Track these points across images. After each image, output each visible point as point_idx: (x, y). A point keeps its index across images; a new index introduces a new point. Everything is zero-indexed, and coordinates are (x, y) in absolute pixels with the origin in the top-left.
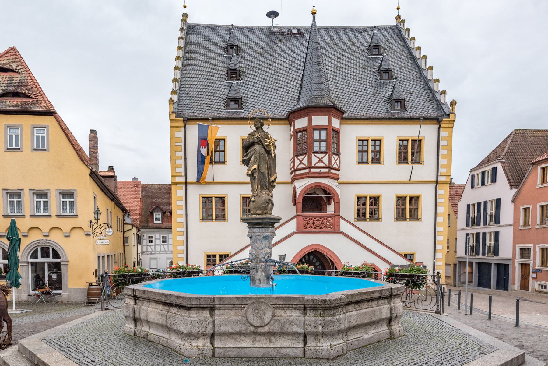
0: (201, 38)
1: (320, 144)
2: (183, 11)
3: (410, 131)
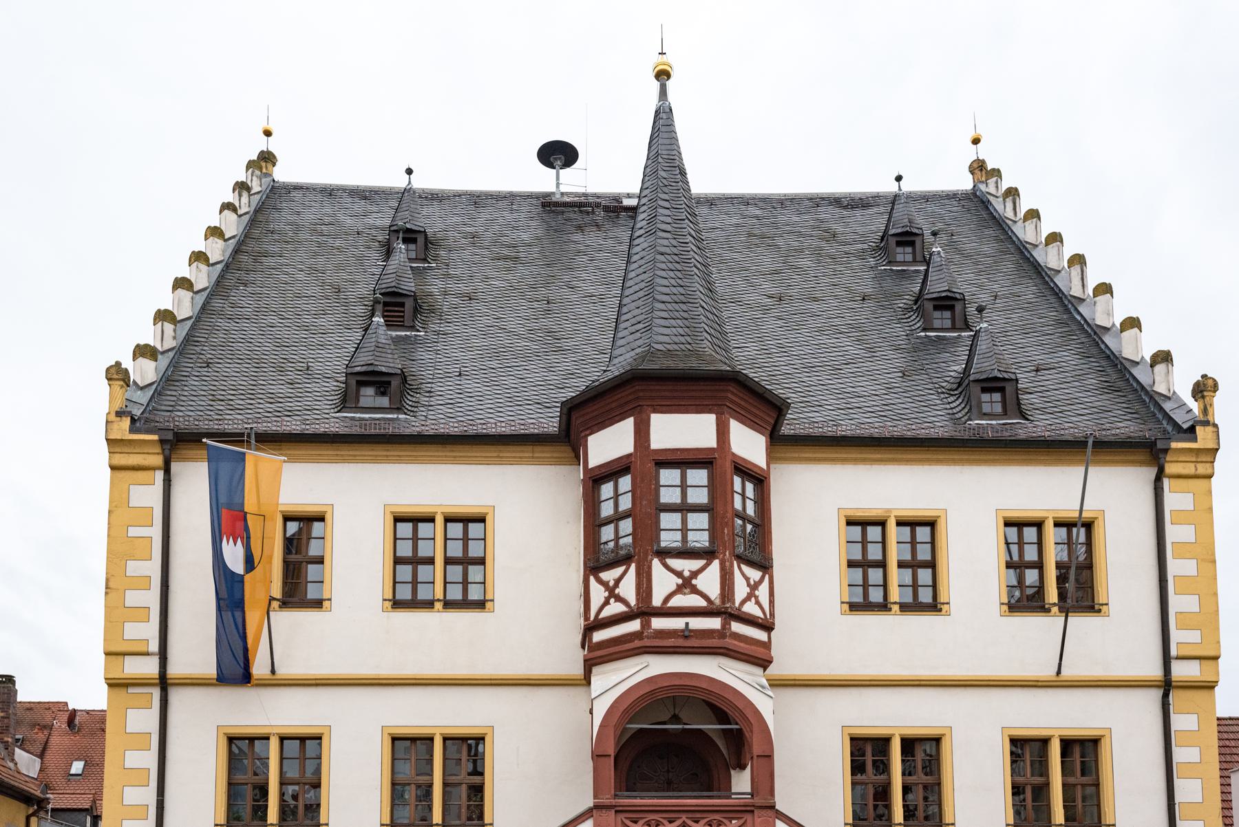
0: (309, 217)
1: (684, 521)
2: (262, 144)
3: (1047, 489)
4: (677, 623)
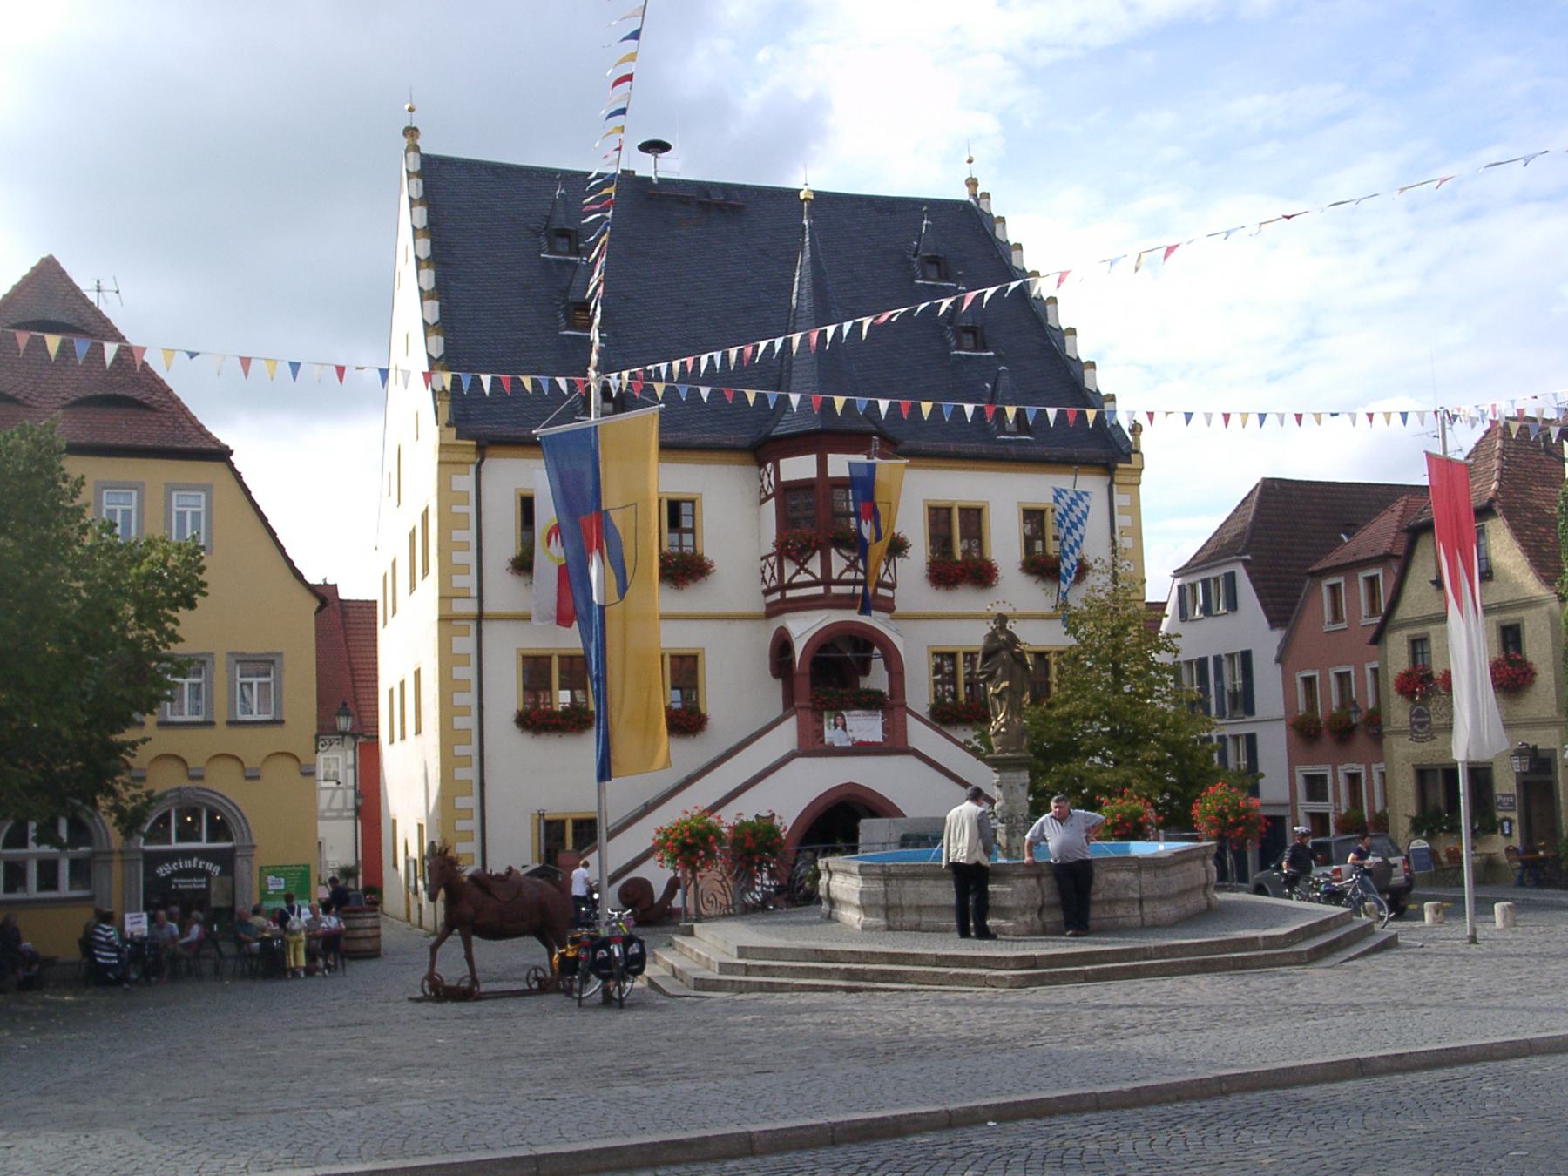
4: (847, 590)
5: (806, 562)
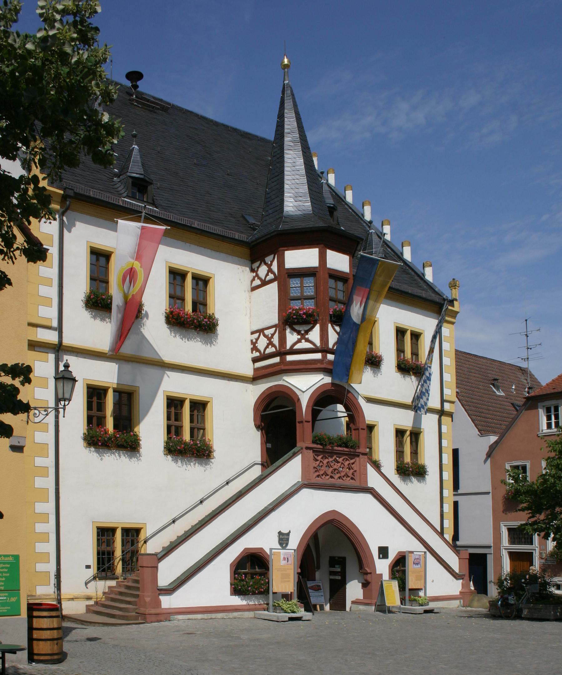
5: (307, 332)
